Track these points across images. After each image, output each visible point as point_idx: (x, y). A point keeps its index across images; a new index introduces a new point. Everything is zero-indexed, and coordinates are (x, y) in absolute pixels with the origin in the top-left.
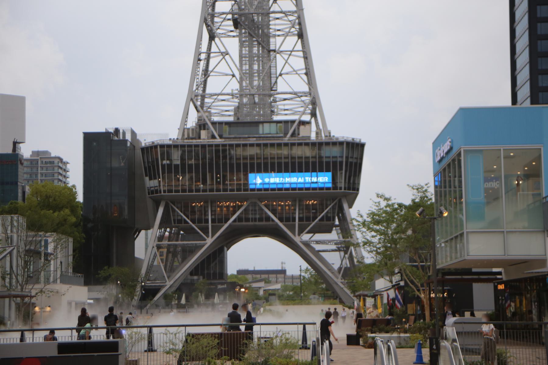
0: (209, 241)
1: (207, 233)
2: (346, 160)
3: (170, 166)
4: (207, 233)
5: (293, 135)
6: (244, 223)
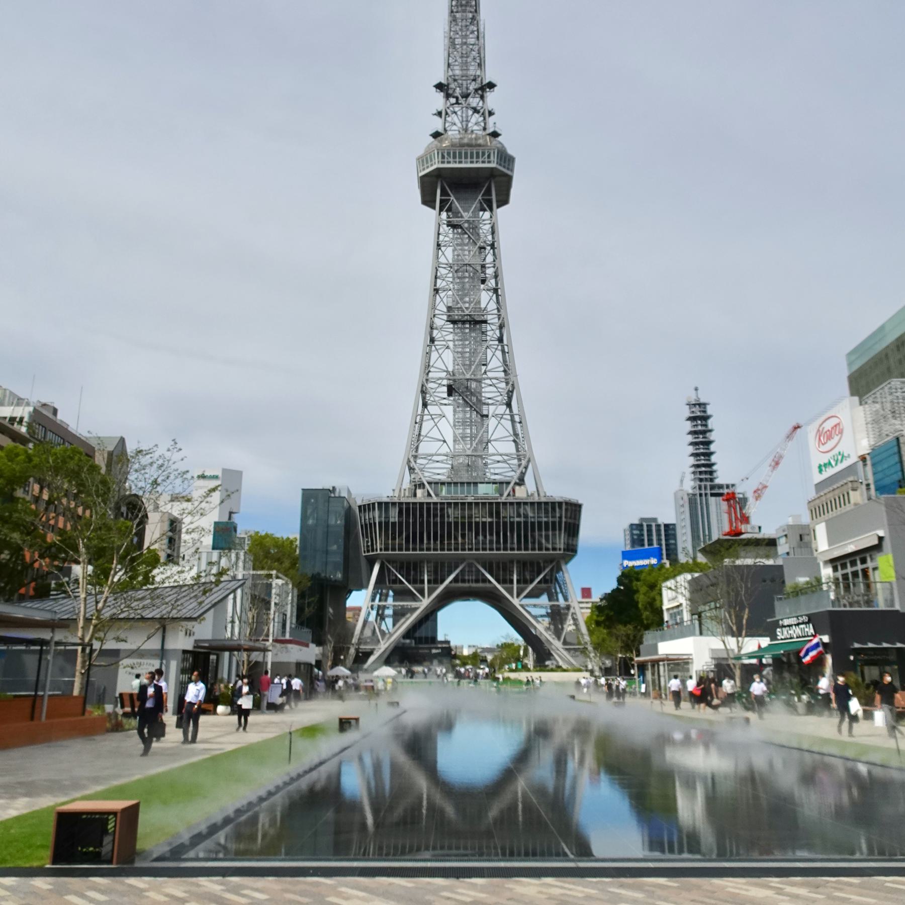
0: (425, 603)
1: (423, 594)
4: (423, 594)
5: (509, 495)
6: (460, 585)
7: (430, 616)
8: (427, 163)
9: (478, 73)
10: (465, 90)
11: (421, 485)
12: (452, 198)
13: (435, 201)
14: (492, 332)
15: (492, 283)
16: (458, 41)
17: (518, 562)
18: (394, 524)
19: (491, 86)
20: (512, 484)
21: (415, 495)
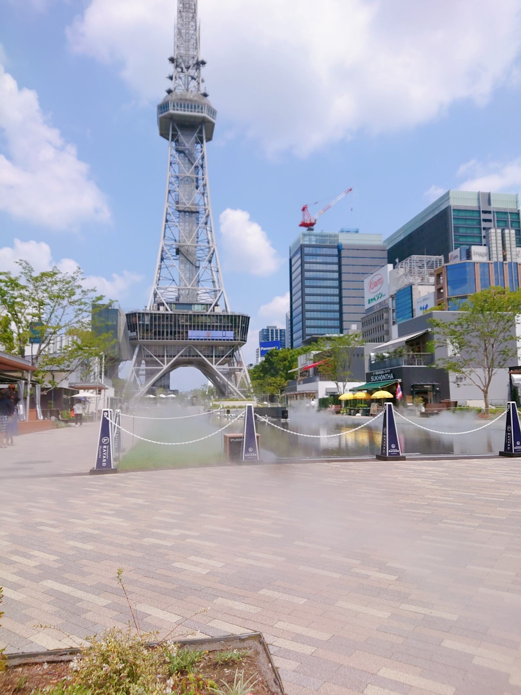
0: (165, 367)
2: (239, 324)
3: (143, 325)
5: (211, 311)
6: (184, 358)
7: (166, 375)
8: (164, 109)
9: (195, 53)
10: (187, 64)
11: (163, 304)
12: (179, 133)
13: (169, 135)
14: (202, 220)
15: (201, 188)
17: (216, 346)
18: (147, 325)
19: (203, 63)
20: (213, 305)
21: (159, 309)
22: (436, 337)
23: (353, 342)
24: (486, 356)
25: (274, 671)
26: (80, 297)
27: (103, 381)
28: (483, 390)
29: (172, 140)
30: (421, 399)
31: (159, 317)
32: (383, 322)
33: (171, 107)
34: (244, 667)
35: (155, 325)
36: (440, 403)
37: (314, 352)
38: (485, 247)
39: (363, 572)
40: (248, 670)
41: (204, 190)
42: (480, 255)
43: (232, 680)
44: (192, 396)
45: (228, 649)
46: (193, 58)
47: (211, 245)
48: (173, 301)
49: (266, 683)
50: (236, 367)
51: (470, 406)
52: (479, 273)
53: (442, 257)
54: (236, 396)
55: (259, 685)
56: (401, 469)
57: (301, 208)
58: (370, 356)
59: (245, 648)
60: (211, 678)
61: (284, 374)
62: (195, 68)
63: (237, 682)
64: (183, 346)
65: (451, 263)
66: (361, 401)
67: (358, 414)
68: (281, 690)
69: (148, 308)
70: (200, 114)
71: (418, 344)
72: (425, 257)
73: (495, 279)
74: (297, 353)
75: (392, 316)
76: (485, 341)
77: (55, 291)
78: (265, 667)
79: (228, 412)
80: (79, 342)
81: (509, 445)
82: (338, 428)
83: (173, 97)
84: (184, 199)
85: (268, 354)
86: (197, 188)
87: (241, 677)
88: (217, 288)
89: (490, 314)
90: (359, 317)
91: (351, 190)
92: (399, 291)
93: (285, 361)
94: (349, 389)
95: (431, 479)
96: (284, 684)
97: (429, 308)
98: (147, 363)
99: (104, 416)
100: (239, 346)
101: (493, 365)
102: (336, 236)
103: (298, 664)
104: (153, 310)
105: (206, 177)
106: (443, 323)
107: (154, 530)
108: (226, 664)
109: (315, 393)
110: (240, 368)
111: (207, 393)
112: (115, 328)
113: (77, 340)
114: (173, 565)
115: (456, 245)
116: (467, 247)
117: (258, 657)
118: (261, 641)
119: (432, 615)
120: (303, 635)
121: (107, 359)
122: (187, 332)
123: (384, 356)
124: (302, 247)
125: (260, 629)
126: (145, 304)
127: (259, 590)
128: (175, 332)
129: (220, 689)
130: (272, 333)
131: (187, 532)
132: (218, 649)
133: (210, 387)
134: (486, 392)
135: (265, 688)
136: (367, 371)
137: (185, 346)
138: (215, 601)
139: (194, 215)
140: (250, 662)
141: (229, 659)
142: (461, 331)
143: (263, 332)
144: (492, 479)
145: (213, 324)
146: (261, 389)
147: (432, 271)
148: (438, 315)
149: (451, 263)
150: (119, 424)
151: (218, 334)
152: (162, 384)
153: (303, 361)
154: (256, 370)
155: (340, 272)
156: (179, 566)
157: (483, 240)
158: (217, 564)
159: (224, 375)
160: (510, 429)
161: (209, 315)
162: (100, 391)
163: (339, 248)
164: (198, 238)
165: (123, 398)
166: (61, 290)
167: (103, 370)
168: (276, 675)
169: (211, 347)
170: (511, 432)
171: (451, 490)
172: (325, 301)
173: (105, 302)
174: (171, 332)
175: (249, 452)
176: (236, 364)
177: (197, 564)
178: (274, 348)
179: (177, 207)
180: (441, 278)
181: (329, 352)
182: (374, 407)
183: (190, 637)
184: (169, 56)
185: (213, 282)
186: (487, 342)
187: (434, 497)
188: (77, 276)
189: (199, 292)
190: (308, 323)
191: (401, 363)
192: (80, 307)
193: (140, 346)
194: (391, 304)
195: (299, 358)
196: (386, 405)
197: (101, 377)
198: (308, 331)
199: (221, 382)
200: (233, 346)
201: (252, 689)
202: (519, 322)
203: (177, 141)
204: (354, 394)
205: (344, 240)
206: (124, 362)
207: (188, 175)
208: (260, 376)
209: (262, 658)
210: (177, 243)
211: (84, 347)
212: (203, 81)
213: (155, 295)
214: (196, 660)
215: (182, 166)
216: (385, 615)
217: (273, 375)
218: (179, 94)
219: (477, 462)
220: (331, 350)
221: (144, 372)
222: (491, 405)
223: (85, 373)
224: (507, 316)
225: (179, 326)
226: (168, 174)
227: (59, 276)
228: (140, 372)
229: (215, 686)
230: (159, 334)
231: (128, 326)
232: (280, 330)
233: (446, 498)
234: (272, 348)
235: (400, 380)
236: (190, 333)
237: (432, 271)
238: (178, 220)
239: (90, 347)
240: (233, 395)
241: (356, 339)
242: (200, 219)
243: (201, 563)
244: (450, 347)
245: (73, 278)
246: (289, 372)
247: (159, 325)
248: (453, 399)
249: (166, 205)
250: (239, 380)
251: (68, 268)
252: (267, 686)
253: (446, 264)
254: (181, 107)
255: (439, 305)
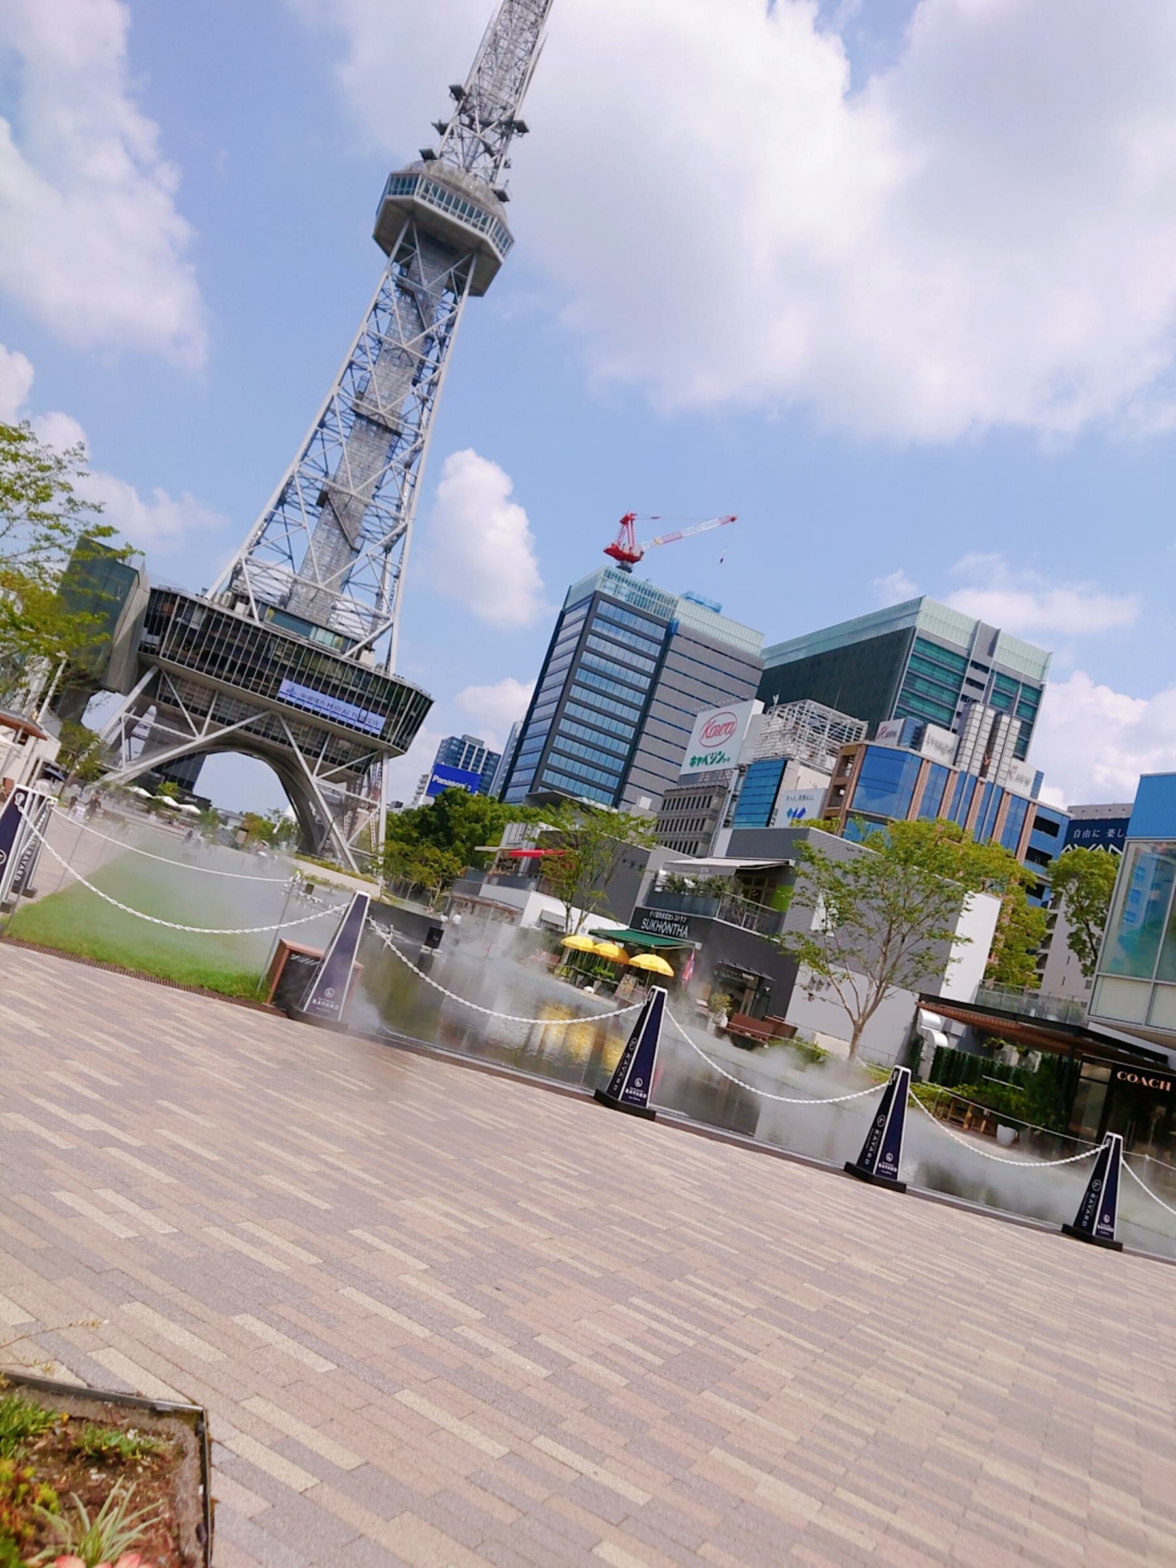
0: (200, 739)
3: (184, 627)
5: (351, 656)
6: (251, 735)
7: (195, 758)
8: (403, 186)
9: (511, 101)
10: (486, 115)
11: (246, 600)
12: (418, 251)
14: (402, 454)
15: (423, 387)
16: (503, 43)
18: (193, 631)
19: (522, 128)
20: (360, 645)
21: (233, 607)
22: (800, 881)
23: (632, 833)
24: (885, 954)
25: (205, 1505)
26: (59, 510)
27: (41, 718)
28: (854, 1022)
29: (396, 260)
30: (728, 998)
31: (227, 625)
32: (706, 812)
33: (419, 189)
34: (138, 1476)
35: (211, 639)
36: (763, 1019)
37: (544, 826)
38: (954, 735)
39: (480, 1340)
40: (146, 1486)
41: (429, 393)
42: (939, 747)
43: (98, 1500)
44: (238, 824)
45: (115, 1424)
46: (505, 109)
47: (402, 515)
48: (274, 601)
49: (175, 1530)
50: (362, 797)
51: (820, 1045)
52: (925, 782)
53: (864, 725)
54: (338, 861)
55: (157, 1530)
56: (637, 1135)
57: (622, 517)
58: (656, 875)
59: (157, 1434)
60: (52, 1482)
61: (463, 850)
62: (499, 131)
63: (111, 1508)
64: (261, 708)
65: (879, 742)
66: (604, 961)
67: (589, 988)
68: (205, 1554)
69: (209, 596)
70: (477, 232)
71: (760, 883)
72: (832, 714)
73: (952, 806)
74: (507, 814)
75: (728, 807)
76: (893, 922)
77: (5, 474)
78: (188, 1491)
79: (309, 889)
80: (18, 609)
81: (870, 1155)
82: (538, 1007)
83: (432, 170)
84: (377, 391)
85: (444, 794)
86: (415, 383)
87: (123, 1499)
88: (384, 612)
89: (919, 873)
90: (662, 786)
91: (733, 520)
92: (758, 762)
93: (476, 822)
94: (588, 931)
95: (689, 1176)
96: (219, 1546)
97: (805, 817)
98: (161, 716)
99: (14, 799)
100: (386, 755)
101: (891, 978)
102: (672, 602)
103: (266, 1504)
104: (219, 603)
105: (443, 368)
106: (823, 859)
107: (38, 1101)
108: (100, 1459)
109: (516, 913)
110: (372, 802)
111: (275, 831)
112: (114, 611)
113: (14, 602)
114: (55, 1194)
115: (900, 711)
116: (920, 723)
117: (178, 1463)
118: (200, 1429)
119: (597, 1479)
120: (298, 1443)
121: (70, 671)
122: (279, 682)
123: (684, 884)
124: (595, 598)
125: (205, 1400)
126: (206, 584)
127: (236, 1314)
128: (252, 670)
129: (62, 1516)
130: (470, 752)
131: (113, 1131)
132: (92, 1418)
133: (286, 820)
134: (858, 1029)
135: (170, 1541)
136: (639, 903)
137: (264, 711)
138: (125, 1307)
139: (388, 435)
140: (156, 1468)
141: (110, 1448)
142: (852, 888)
143: (452, 743)
144: (813, 1216)
145: (345, 686)
146: (402, 864)
147: (837, 745)
148: (819, 840)
149: (879, 742)
150: (42, 830)
151: (349, 712)
152: (178, 775)
153: (512, 836)
154: (406, 820)
155: (655, 678)
156: (69, 1203)
157: (956, 721)
158: (159, 1226)
159: (330, 804)
160: (883, 1123)
161: (344, 664)
162: (25, 737)
163: (671, 630)
164: (378, 488)
165: (73, 772)
166: (20, 477)
167: (50, 693)
168: (205, 1518)
169: (323, 734)
170: (882, 1130)
171: (725, 1216)
172: (605, 726)
173: (115, 543)
174: (243, 666)
175: (323, 996)
176: (364, 791)
177: (112, 1211)
178: (463, 786)
179: (357, 405)
180: (850, 766)
181: (576, 837)
182: (628, 983)
183: (36, 1372)
184: (454, 83)
185: (379, 595)
186: (894, 926)
187: (684, 1218)
188: (70, 462)
189: (339, 606)
190: (554, 759)
191: (713, 910)
192: (49, 532)
193: (160, 671)
194: (734, 782)
195: (508, 827)
196: (654, 990)
197: (39, 707)
198: (548, 776)
199: (318, 818)
200: (373, 750)
201: (140, 1536)
202: (968, 907)
203: (407, 266)
204: (595, 944)
205: (686, 616)
206: (108, 693)
207: (405, 346)
208: (410, 835)
209: (189, 1468)
210: (327, 481)
211: (26, 624)
212: (507, 165)
213: (237, 572)
214: (32, 1428)
215: (399, 322)
216: (497, 1449)
217: (438, 844)
218: (446, 169)
219: (794, 1171)
220: (583, 833)
221: (146, 733)
222: (861, 1057)
223: (6, 683)
224: (951, 888)
225: (266, 660)
226: (364, 326)
227: (28, 447)
228: (136, 730)
229: (53, 1506)
230: (213, 661)
231: (148, 616)
232: (489, 753)
233: (707, 1228)
234: (459, 785)
235: (698, 946)
236: (286, 684)
237: (837, 745)
238: (348, 432)
239: (38, 630)
240: (335, 856)
241: (641, 830)
242: (397, 450)
243: (123, 1212)
244: (821, 913)
245: (59, 462)
246: (477, 848)
247: (221, 642)
248: (790, 1020)
249: (331, 390)
250: (360, 827)
251: (57, 435)
252: (176, 1538)
253: (867, 742)
254: (441, 198)
255: (828, 818)
